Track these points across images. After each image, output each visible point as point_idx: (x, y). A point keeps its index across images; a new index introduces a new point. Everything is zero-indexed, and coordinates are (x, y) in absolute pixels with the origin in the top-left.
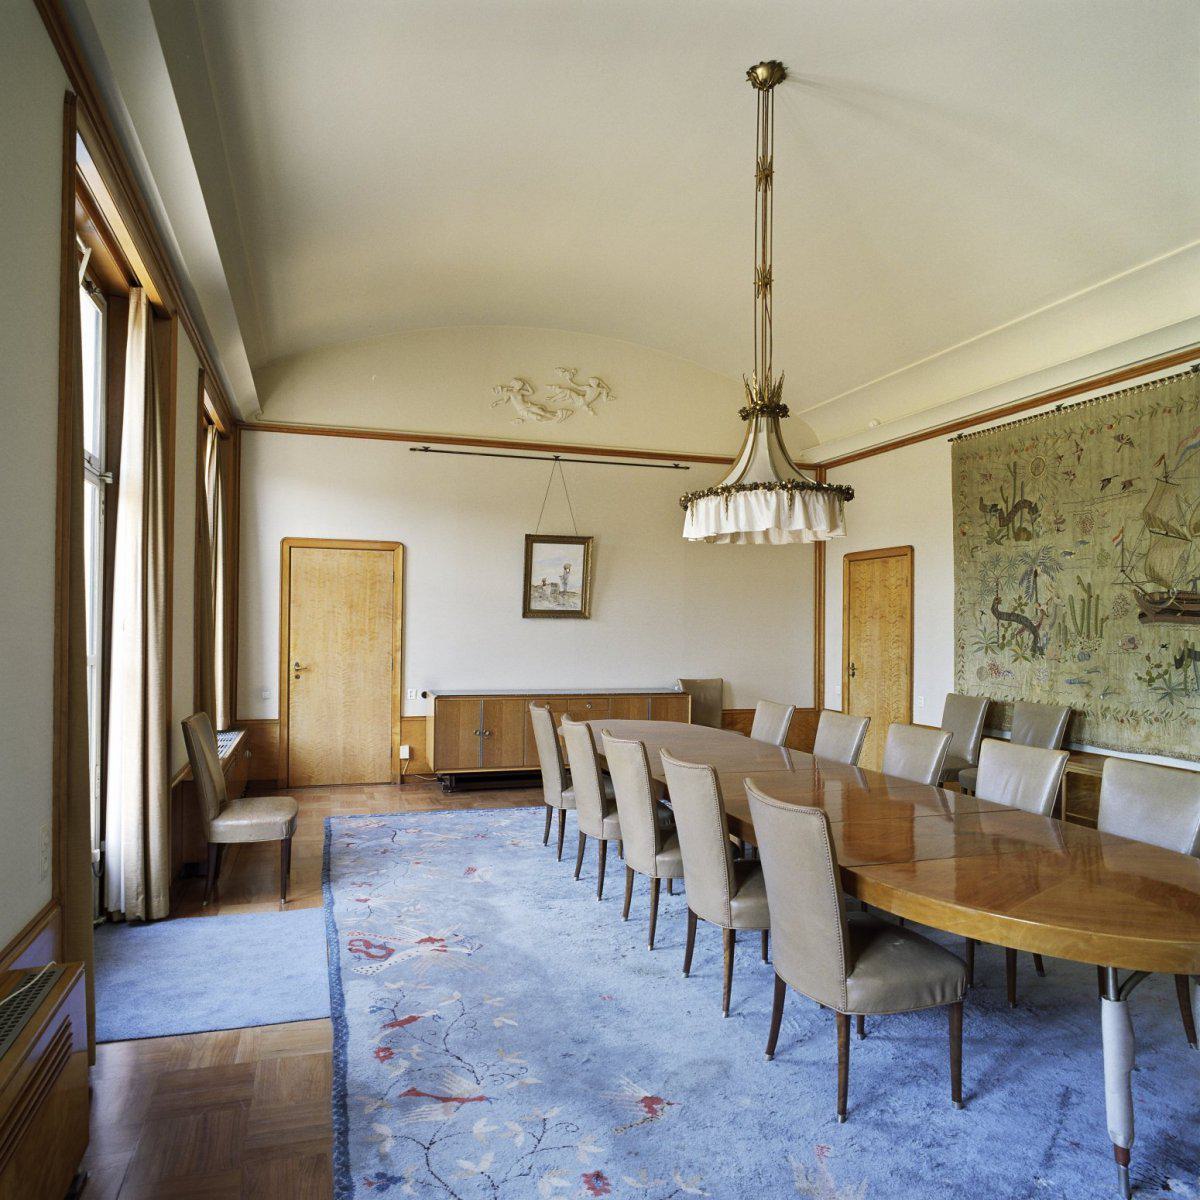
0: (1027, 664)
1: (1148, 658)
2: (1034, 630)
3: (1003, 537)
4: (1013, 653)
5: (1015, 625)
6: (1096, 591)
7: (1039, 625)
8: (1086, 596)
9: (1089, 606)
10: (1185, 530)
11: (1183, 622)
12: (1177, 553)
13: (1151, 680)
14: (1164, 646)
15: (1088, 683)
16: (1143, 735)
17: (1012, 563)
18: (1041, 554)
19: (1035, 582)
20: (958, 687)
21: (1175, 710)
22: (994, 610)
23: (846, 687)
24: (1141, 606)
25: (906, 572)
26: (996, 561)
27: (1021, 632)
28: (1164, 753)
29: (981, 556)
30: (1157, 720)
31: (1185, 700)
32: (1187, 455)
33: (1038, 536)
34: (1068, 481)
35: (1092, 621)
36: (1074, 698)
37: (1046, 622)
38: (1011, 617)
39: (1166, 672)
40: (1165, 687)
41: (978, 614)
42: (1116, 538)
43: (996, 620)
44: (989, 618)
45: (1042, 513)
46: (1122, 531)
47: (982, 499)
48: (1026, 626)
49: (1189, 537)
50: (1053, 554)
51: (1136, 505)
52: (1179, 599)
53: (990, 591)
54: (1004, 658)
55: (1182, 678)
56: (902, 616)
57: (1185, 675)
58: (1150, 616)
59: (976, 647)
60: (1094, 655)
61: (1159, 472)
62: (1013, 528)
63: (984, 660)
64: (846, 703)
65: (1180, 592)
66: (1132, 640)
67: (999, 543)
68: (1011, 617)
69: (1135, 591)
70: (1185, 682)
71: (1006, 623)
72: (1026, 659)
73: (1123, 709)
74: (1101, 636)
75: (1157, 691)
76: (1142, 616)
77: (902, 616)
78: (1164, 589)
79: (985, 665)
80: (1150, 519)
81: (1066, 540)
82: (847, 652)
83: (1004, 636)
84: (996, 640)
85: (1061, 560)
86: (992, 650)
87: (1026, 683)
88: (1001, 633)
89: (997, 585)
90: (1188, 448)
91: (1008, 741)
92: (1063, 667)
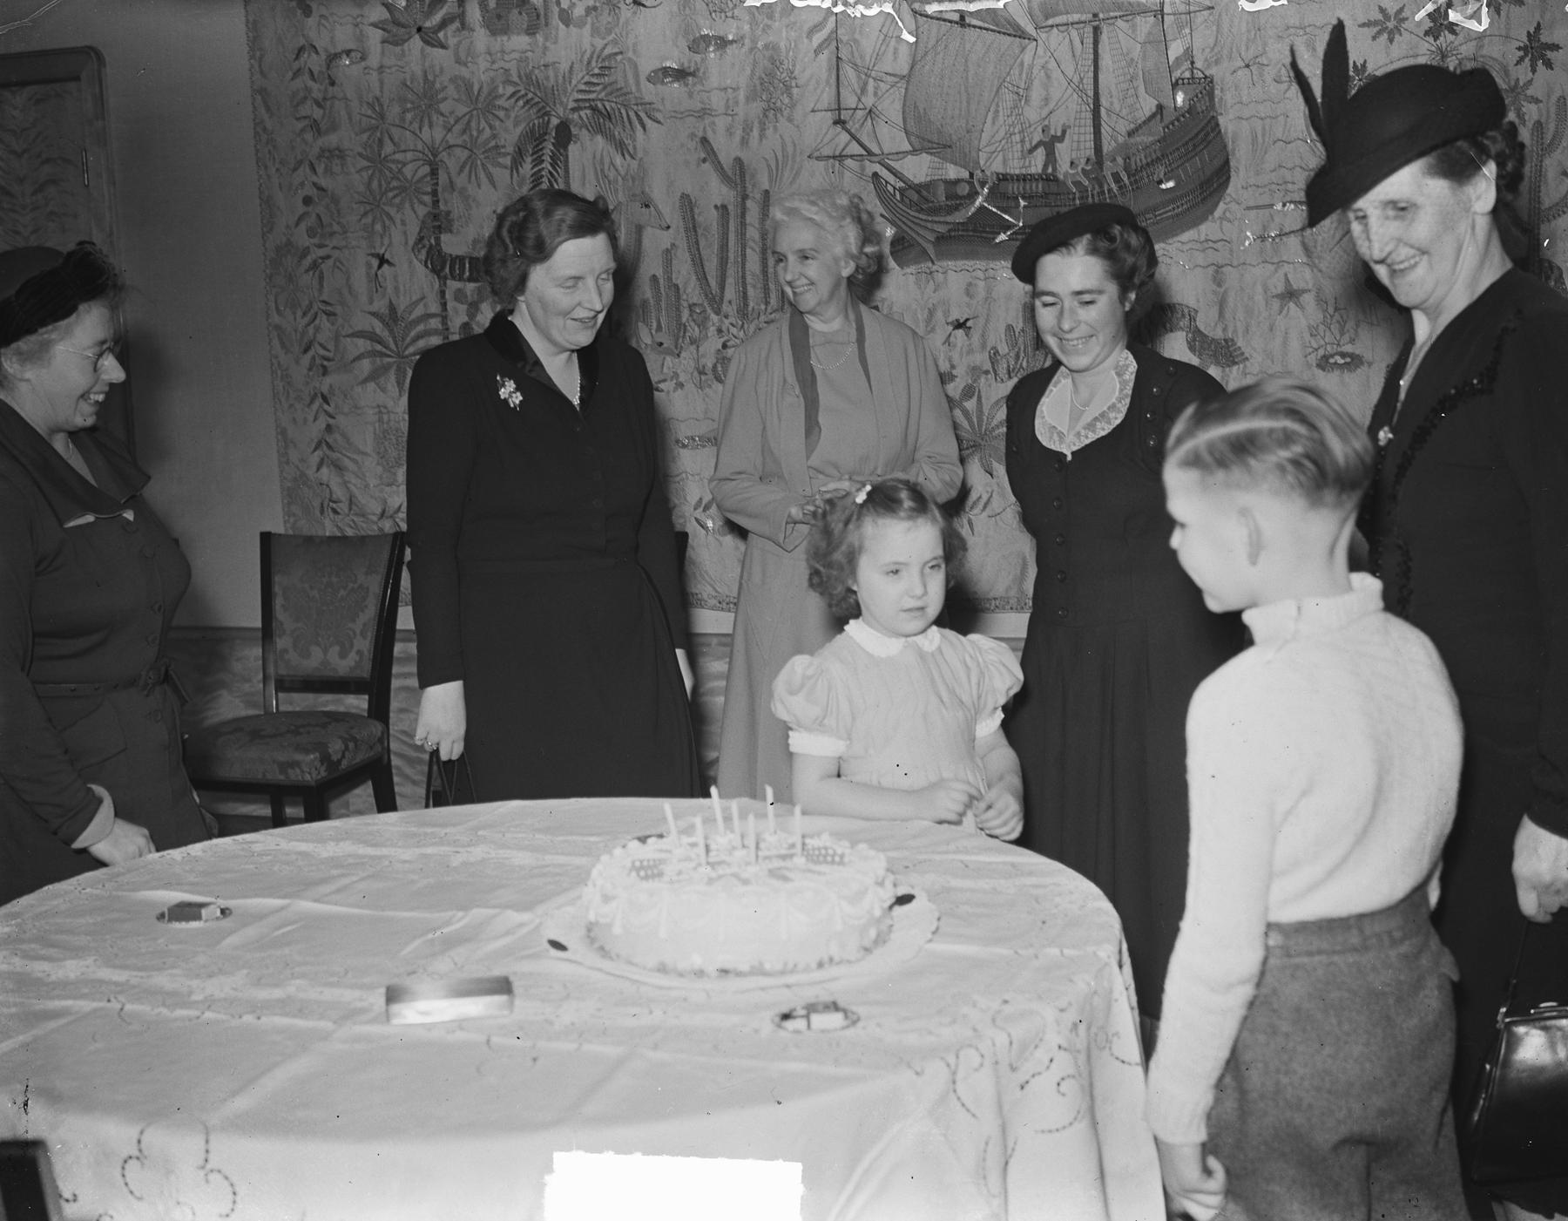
3: (443, 24)
9: (743, 224)
14: (959, 325)
39: (969, 392)
52: (1005, 196)
78: (953, 172)
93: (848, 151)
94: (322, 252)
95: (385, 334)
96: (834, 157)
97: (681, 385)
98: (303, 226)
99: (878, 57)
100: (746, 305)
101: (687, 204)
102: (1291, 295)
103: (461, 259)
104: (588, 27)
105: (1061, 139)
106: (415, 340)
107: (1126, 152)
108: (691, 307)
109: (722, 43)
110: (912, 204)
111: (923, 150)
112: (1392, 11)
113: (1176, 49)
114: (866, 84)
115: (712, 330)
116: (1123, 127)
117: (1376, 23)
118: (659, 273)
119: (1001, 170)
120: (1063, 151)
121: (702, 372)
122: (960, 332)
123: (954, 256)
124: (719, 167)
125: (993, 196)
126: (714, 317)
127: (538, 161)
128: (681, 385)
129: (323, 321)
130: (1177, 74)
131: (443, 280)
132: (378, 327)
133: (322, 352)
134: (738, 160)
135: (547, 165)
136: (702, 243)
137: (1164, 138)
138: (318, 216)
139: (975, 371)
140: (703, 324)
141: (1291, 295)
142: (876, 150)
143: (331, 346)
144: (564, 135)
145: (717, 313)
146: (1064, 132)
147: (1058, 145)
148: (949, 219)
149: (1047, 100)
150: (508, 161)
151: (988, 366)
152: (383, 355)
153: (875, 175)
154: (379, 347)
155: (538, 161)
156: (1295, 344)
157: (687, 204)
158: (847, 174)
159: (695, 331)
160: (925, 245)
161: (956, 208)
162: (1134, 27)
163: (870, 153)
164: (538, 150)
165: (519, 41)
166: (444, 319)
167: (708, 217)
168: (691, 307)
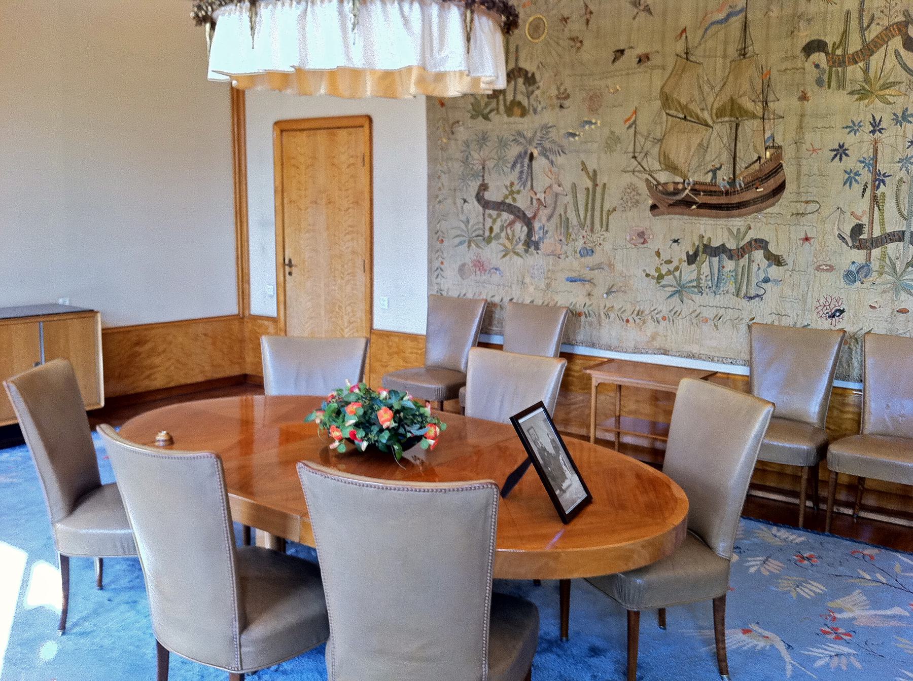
0: (518, 261)
1: (658, 254)
2: (529, 223)
3: (491, 111)
4: (502, 248)
5: (506, 216)
6: (602, 179)
7: (534, 217)
8: (589, 184)
9: (594, 195)
10: (706, 115)
11: (698, 215)
12: (696, 140)
13: (660, 277)
14: (676, 241)
15: (590, 281)
16: (649, 334)
17: (502, 144)
18: (539, 134)
19: (530, 166)
20: (436, 287)
21: (686, 308)
22: (479, 198)
23: (282, 288)
24: (653, 196)
25: (363, 148)
26: (483, 139)
27: (512, 223)
28: (671, 353)
29: (462, 133)
30: (664, 319)
31: (697, 298)
32: (709, 32)
33: (535, 111)
34: (574, 49)
35: (597, 213)
36: (572, 296)
37: (543, 214)
38: (500, 206)
39: (677, 269)
40: (675, 284)
41: (459, 202)
42: (629, 119)
43: (481, 209)
44: (474, 207)
45: (541, 84)
46: (635, 112)
48: (518, 217)
49: (711, 123)
50: (553, 134)
51: (652, 81)
52: (695, 190)
53: (475, 175)
54: (491, 253)
55: (694, 276)
56: (357, 203)
57: (699, 272)
58: (662, 208)
59: (457, 240)
60: (598, 250)
61: (680, 47)
62: (505, 100)
63: (467, 255)
64: (282, 307)
65: (696, 183)
66: (641, 235)
67: (486, 118)
68: (500, 206)
69: (647, 180)
70: (698, 279)
71: (494, 213)
72: (517, 254)
73: (629, 308)
74: (607, 230)
75: (666, 289)
76: (654, 207)
77: (357, 203)
79: (468, 261)
80: (667, 99)
81: (567, 119)
82: (282, 245)
83: (491, 229)
84: (481, 232)
85: (565, 142)
86: (477, 245)
87: (518, 278)
88: (489, 223)
89: (483, 168)
90: (713, 23)
91: (500, 347)
92: (563, 263)
93: (637, 169)
111: (666, 170)
112: (856, 123)
116: (744, 165)
121: (576, 252)
124: (588, 173)
150: (509, 165)
165: (516, 119)
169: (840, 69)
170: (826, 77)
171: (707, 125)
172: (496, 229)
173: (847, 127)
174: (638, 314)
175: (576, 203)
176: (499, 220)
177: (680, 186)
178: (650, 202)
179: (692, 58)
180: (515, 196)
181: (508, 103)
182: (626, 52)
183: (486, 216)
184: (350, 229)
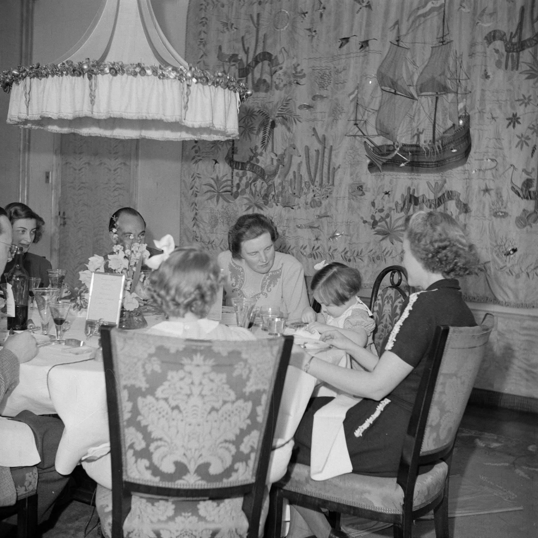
1: (373, 204)
6: (330, 142)
8: (319, 147)
9: (323, 156)
10: (413, 90)
13: (375, 224)
14: (387, 193)
19: (271, 132)
27: (255, 180)
39: (388, 216)
47: (220, 48)
49: (416, 96)
52: (404, 151)
59: (209, 194)
78: (390, 142)
80: (382, 78)
83: (238, 186)
84: (229, 188)
88: (236, 180)
94: (199, 158)
95: (214, 185)
96: (353, 136)
97: (300, 208)
98: (194, 149)
99: (369, 103)
100: (322, 183)
101: (307, 149)
102: (487, 190)
103: (239, 163)
104: (284, 91)
105: (422, 133)
106: (223, 188)
107: (442, 138)
108: (305, 182)
109: (322, 97)
110: (376, 153)
112: (527, 97)
113: (461, 106)
114: (365, 112)
115: (311, 190)
116: (442, 130)
117: (521, 100)
118: (296, 171)
119: (404, 143)
120: (423, 138)
121: (307, 204)
122: (387, 195)
123: (387, 170)
125: (401, 151)
126: (312, 186)
127: (265, 133)
128: (300, 208)
129: (197, 180)
130: (460, 114)
131: (233, 169)
132: (213, 182)
133: (196, 190)
134: (324, 136)
135: (267, 134)
136: (310, 163)
137: (455, 135)
138: (199, 147)
139: (390, 209)
140: (308, 189)
141: (487, 190)
142: (366, 134)
143: (199, 188)
144: (273, 125)
145: (313, 185)
146: (423, 131)
147: (421, 135)
148: (386, 158)
149: (419, 120)
151: (394, 207)
152: (214, 192)
153: (365, 142)
154: (213, 189)
155: (265, 133)
156: (487, 207)
157: (307, 149)
158: (357, 142)
159: (305, 190)
160: (378, 165)
161: (389, 154)
162: (447, 97)
163: (364, 135)
164: (265, 129)
165: (262, 94)
166: (232, 181)
167: (313, 153)
168: (305, 182)
169: (515, 54)
170: (503, 60)
171: (412, 98)
172: (242, 187)
173: (518, 100)
174: (357, 255)
175: (308, 163)
176: (244, 178)
177: (391, 148)
178: (368, 161)
179: (401, 44)
180: (259, 157)
181: (256, 82)
182: (350, 40)
183: (234, 174)
184: (118, 186)
